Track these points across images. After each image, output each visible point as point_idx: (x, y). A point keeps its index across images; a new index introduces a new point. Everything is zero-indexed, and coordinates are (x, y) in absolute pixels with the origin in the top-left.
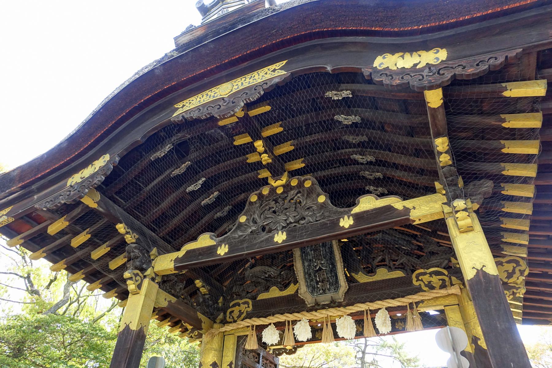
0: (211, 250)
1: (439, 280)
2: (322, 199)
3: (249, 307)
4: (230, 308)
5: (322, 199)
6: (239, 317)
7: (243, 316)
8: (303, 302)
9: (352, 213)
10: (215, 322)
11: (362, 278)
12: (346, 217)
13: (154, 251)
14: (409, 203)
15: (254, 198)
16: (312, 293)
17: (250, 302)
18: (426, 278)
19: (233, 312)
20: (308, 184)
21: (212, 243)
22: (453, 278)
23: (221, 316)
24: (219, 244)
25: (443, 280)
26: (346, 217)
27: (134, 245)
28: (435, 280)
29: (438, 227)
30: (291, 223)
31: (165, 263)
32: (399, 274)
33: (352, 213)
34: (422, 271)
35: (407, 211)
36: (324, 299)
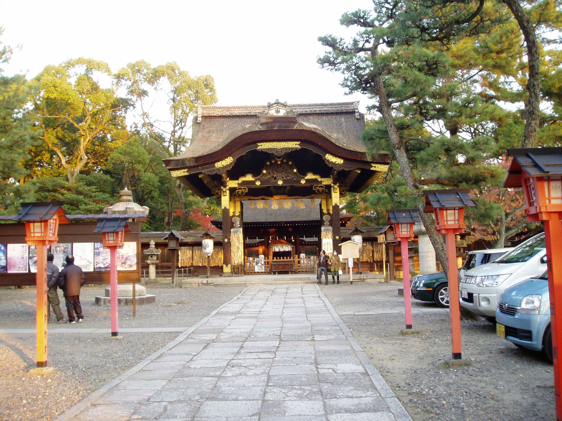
0: (253, 183)
5: (295, 171)
14: (322, 179)
15: (268, 163)
20: (290, 163)
21: (253, 179)
23: (234, 194)
24: (256, 180)
35: (321, 182)
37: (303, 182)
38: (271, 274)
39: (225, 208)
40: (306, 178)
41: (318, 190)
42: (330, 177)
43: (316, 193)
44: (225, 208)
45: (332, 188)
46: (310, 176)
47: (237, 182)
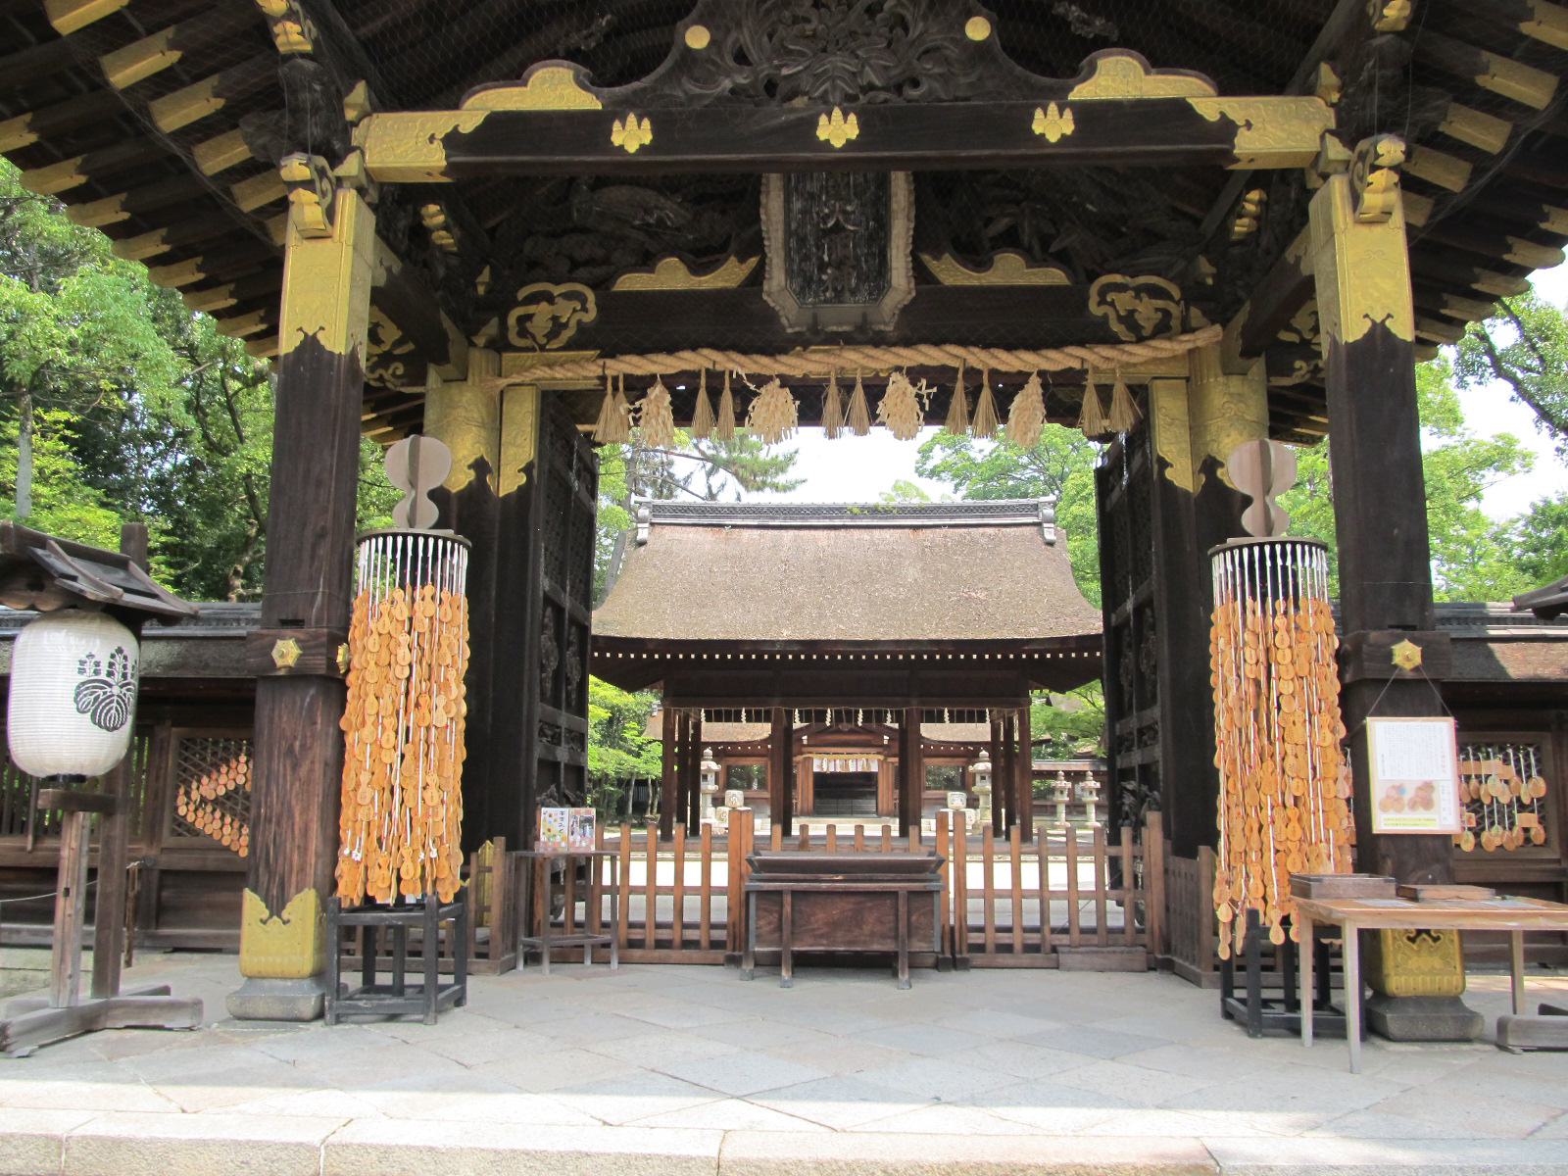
0: (593, 127)
1: (1157, 310)
2: (978, 30)
3: (584, 309)
4: (517, 304)
5: (978, 30)
6: (552, 335)
7: (567, 335)
8: (770, 316)
9: (1073, 96)
10: (472, 344)
11: (951, 273)
12: (1053, 107)
13: (359, 93)
14: (1236, 108)
16: (801, 294)
17: (591, 296)
18: (1124, 301)
19: (529, 317)
21: (588, 102)
22: (1195, 312)
23: (492, 328)
25: (1167, 313)
26: (1053, 107)
27: (310, 65)
28: (1147, 311)
29: (1290, 190)
30: (871, 87)
31: (409, 143)
32: (1054, 276)
33: (1073, 96)
34: (1118, 278)
35: (1227, 129)
36: (842, 315)
37: (1052, 125)
38: (734, 961)
39: (310, 345)
40: (1081, 92)
41: (1129, 320)
42: (1308, 90)
43: (1114, 341)
44: (310, 344)
45: (1338, 186)
46: (1117, 78)
47: (442, 122)
